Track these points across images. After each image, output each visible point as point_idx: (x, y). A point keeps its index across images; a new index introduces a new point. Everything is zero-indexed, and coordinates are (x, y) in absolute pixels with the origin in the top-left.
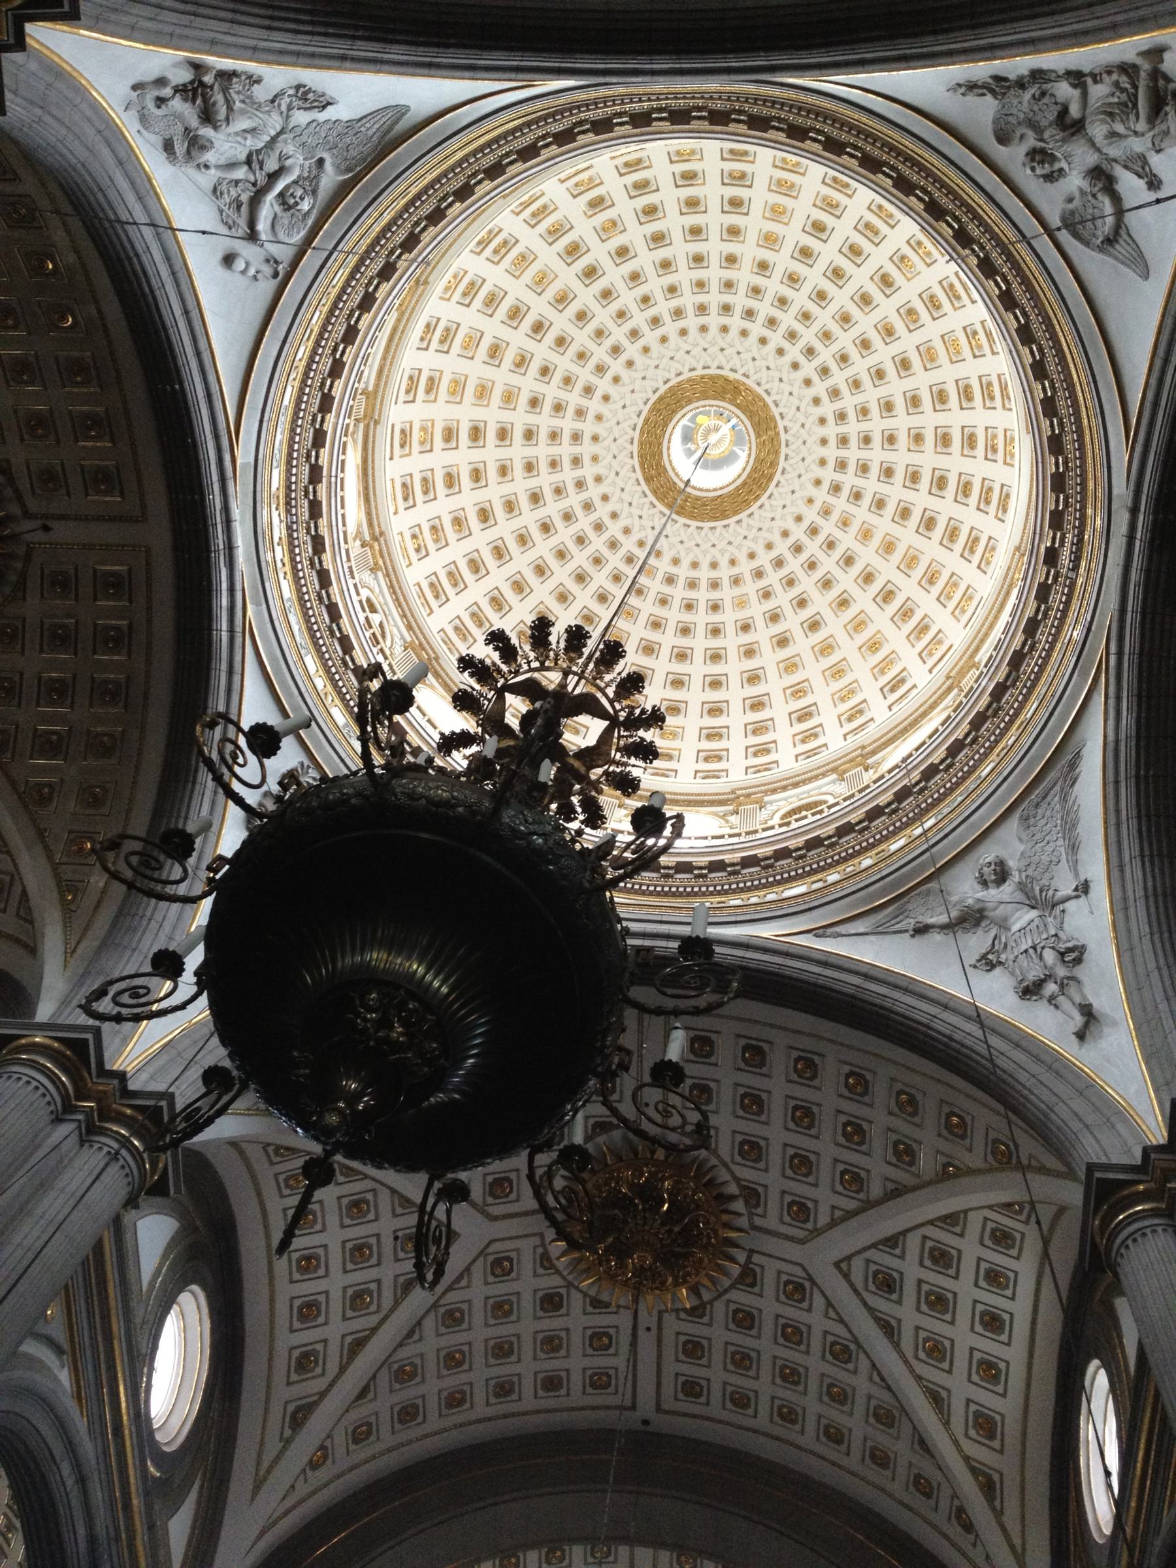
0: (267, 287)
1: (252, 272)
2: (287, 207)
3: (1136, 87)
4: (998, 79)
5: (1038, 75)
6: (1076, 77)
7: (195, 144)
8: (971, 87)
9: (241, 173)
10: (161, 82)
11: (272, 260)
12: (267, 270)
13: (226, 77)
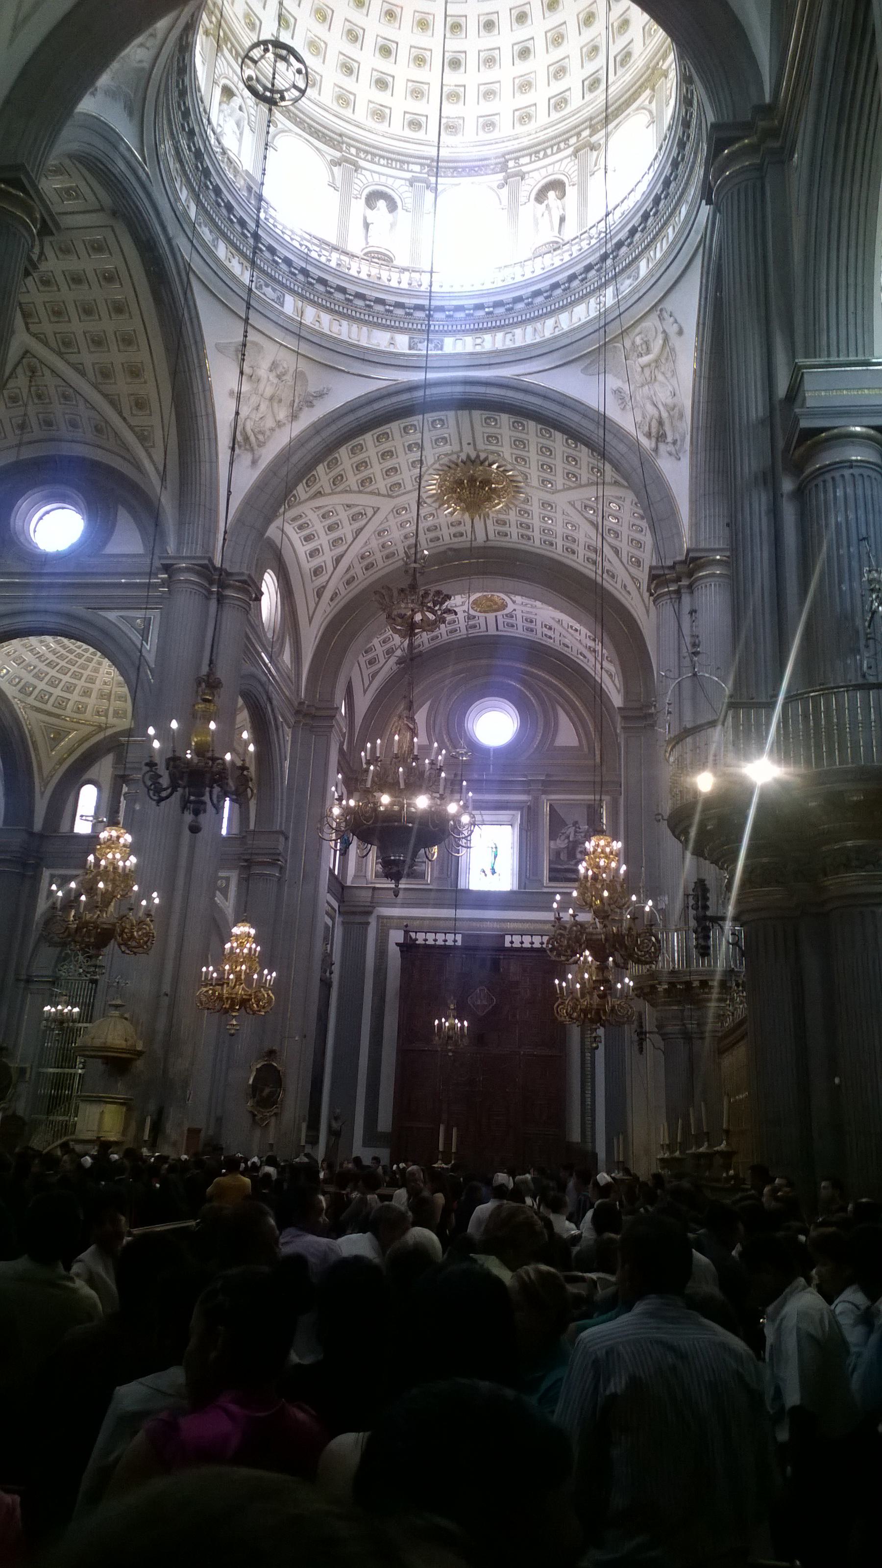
0: (668, 305)
1: (672, 320)
2: (647, 343)
3: (257, 438)
4: (312, 406)
5: (294, 417)
6: (280, 425)
7: (671, 409)
8: (321, 395)
9: (660, 377)
10: (670, 454)
11: (661, 318)
12: (666, 315)
13: (649, 435)
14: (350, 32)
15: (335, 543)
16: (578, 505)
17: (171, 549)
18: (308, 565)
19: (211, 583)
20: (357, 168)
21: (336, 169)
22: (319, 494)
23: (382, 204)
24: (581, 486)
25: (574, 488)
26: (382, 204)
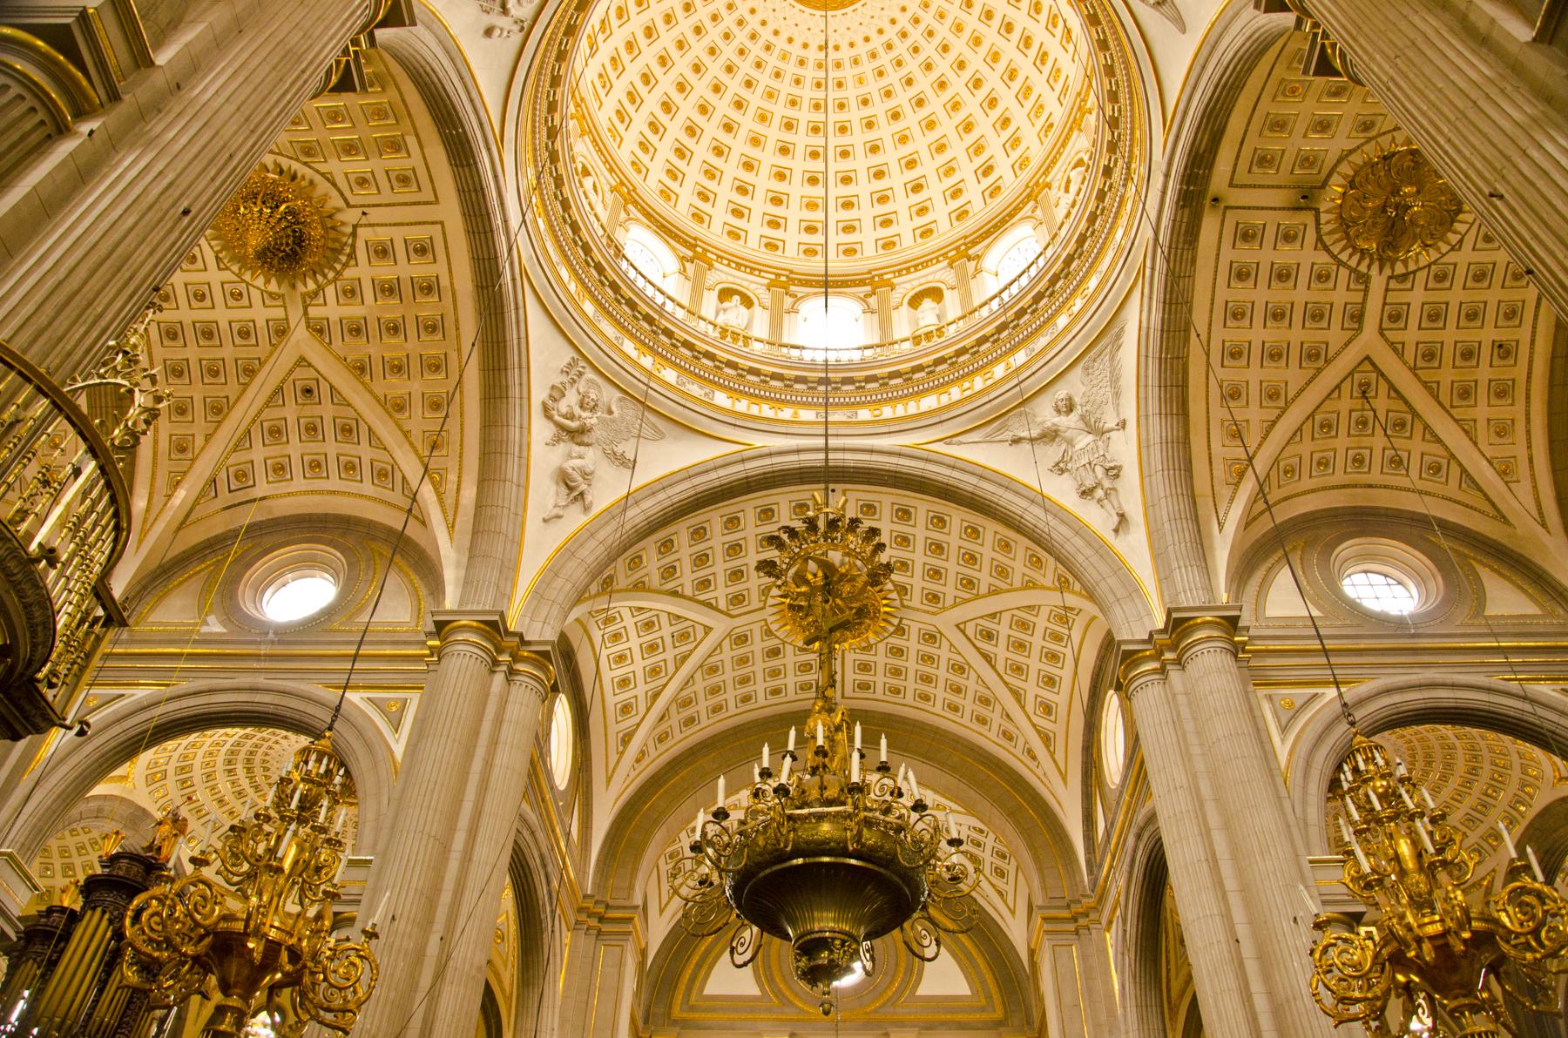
14: (706, 172)
15: (655, 671)
16: (970, 631)
17: (450, 602)
18: (613, 700)
19: (500, 651)
20: (711, 267)
21: (688, 265)
22: (639, 587)
23: (736, 298)
24: (978, 597)
25: (969, 600)
26: (736, 298)
